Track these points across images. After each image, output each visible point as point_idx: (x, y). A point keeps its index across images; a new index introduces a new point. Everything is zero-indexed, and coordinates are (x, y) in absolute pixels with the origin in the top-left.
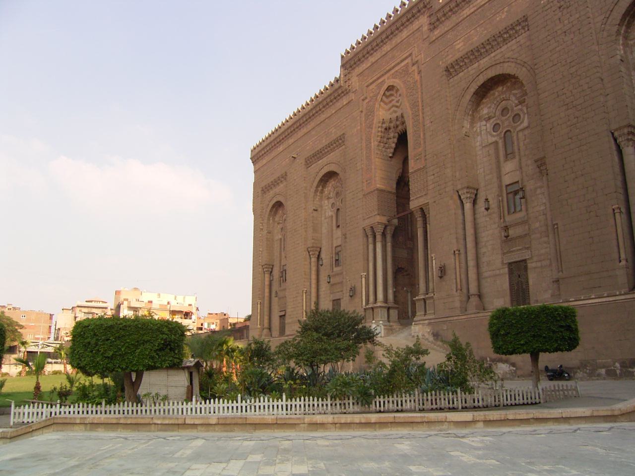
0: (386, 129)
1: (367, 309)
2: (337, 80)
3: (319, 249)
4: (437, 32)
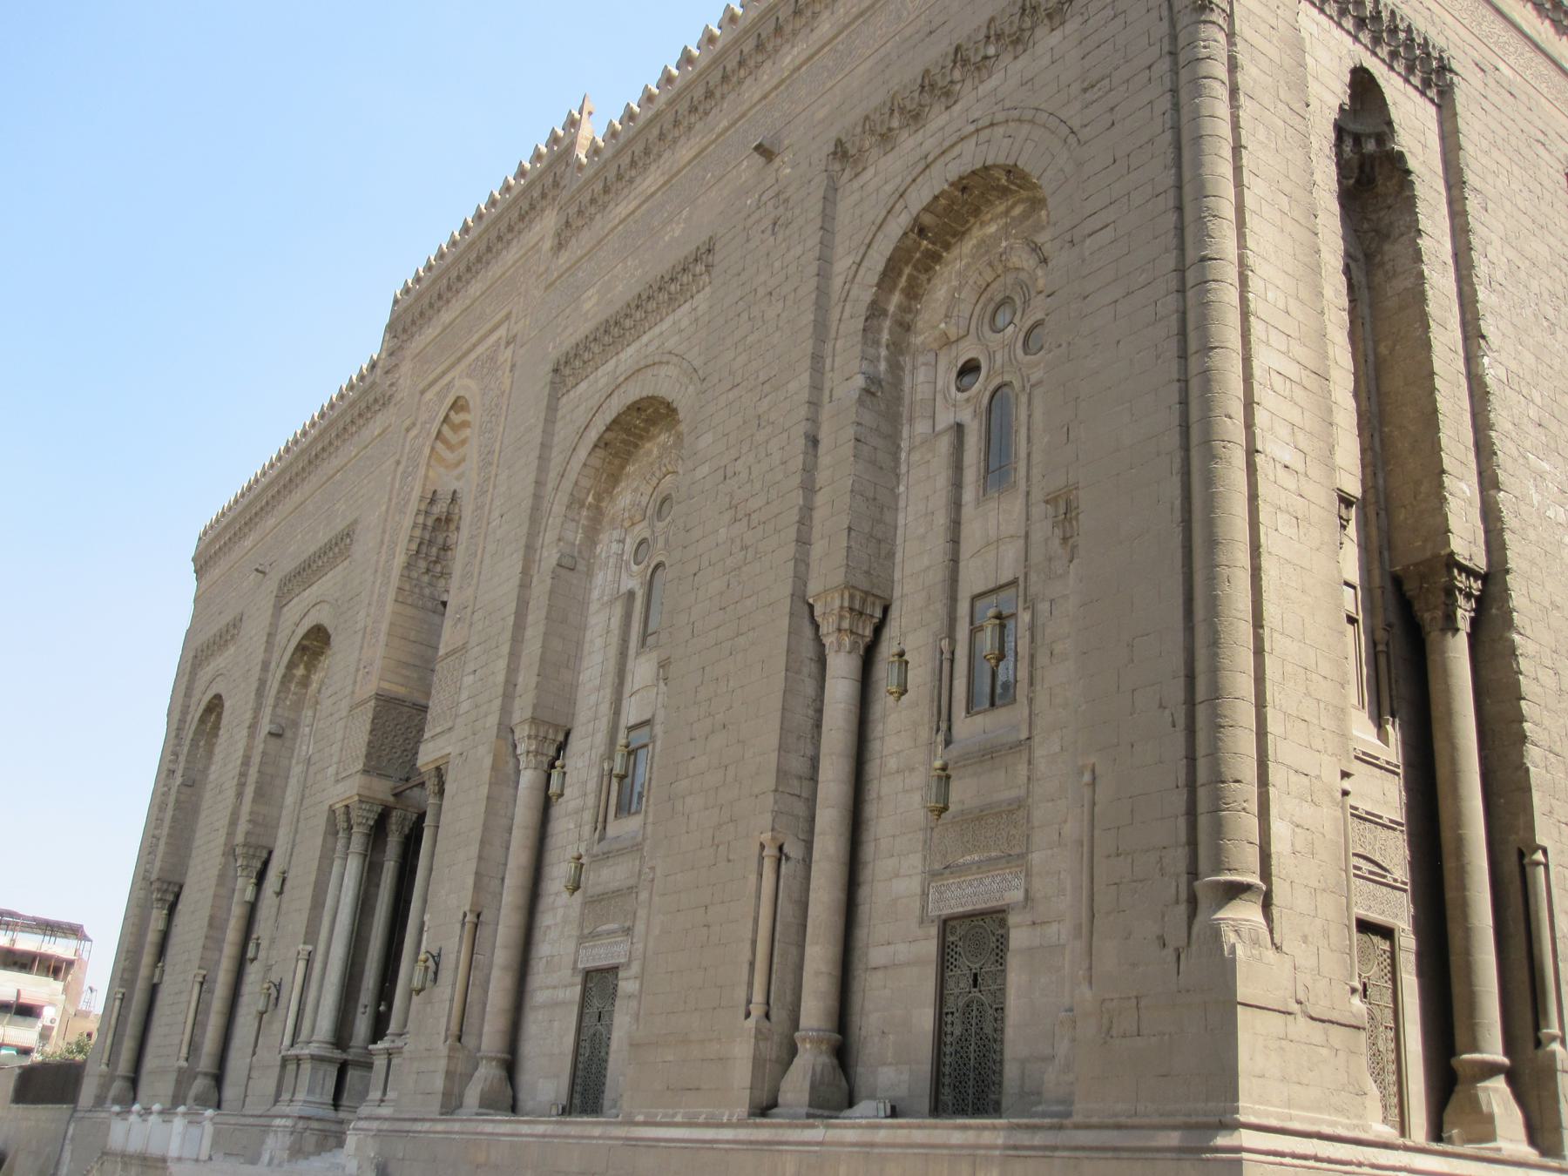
0: (438, 520)
1: (298, 1059)
3: (265, 854)
4: (564, 258)
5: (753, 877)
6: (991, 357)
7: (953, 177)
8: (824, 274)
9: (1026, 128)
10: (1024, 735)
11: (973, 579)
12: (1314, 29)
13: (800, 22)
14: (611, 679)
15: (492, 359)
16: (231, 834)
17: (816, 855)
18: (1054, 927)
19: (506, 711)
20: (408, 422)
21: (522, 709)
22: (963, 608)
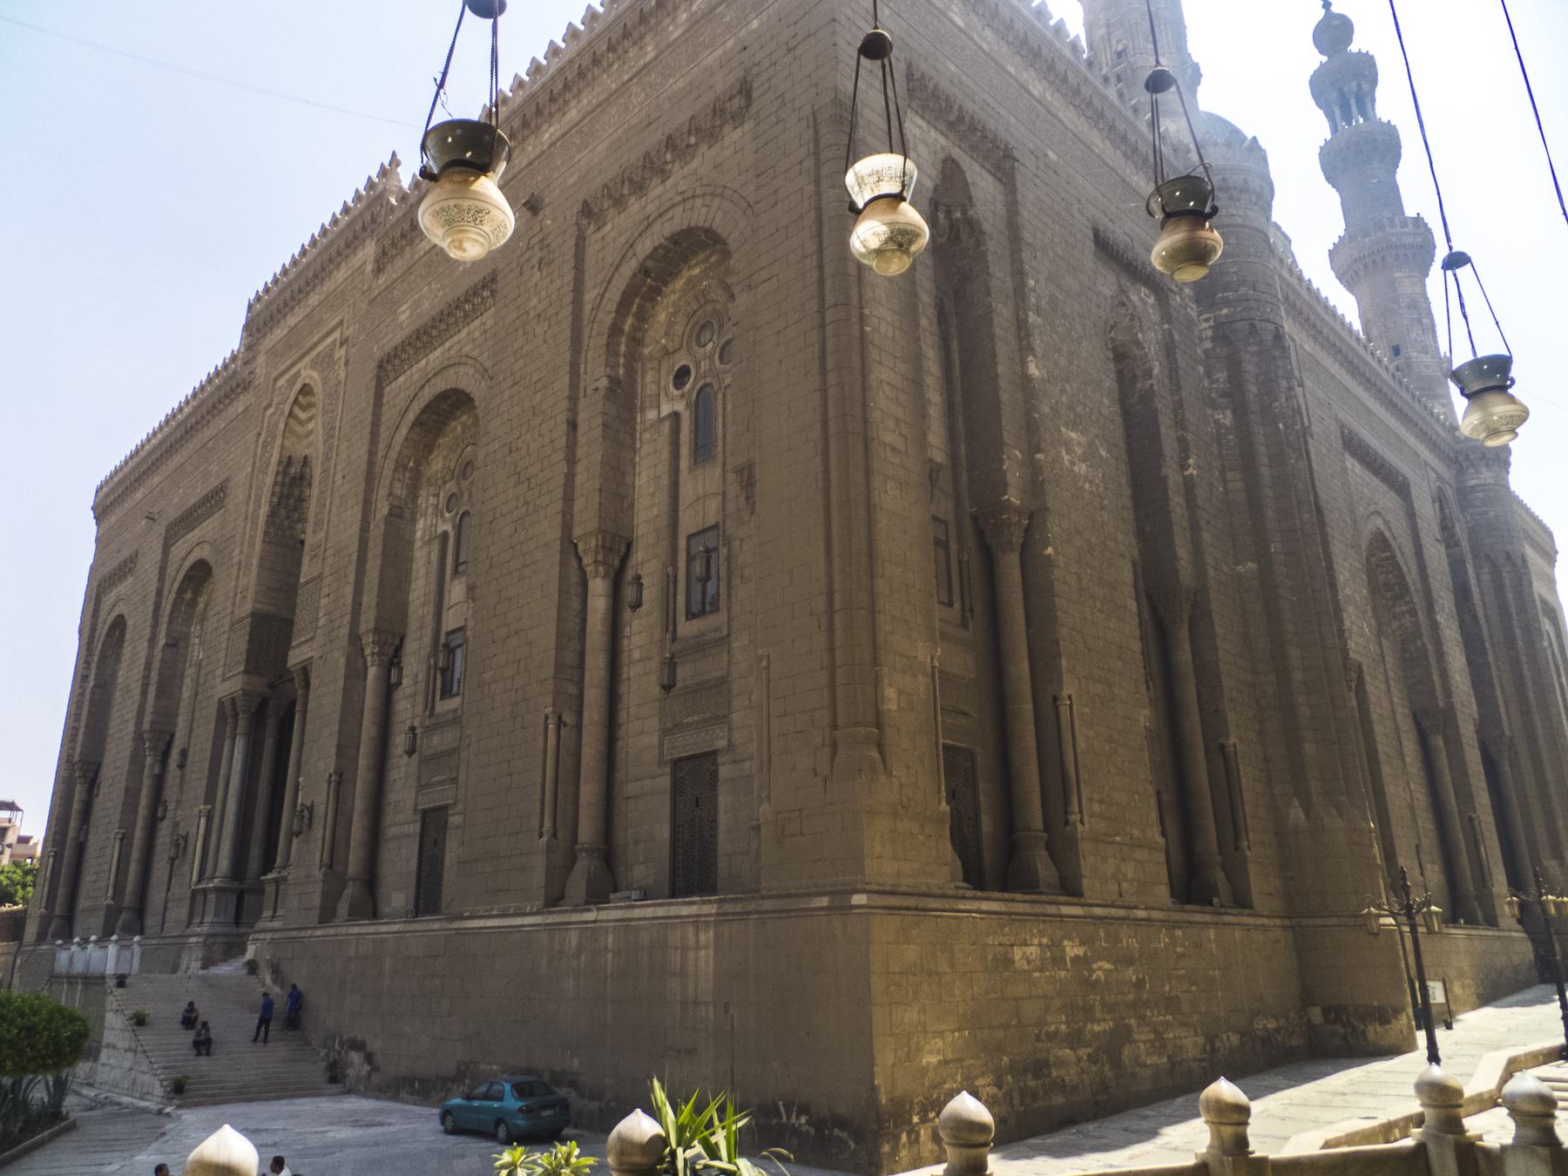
1: (205, 891)
2: (234, 358)
4: (382, 280)
5: (541, 739)
6: (697, 365)
7: (667, 233)
8: (577, 302)
9: (717, 201)
10: (725, 633)
11: (688, 524)
12: (917, 132)
13: (554, 107)
14: (432, 597)
15: (331, 356)
16: (139, 722)
17: (585, 722)
18: (747, 764)
19: (354, 623)
20: (265, 403)
21: (368, 621)
22: (682, 543)
